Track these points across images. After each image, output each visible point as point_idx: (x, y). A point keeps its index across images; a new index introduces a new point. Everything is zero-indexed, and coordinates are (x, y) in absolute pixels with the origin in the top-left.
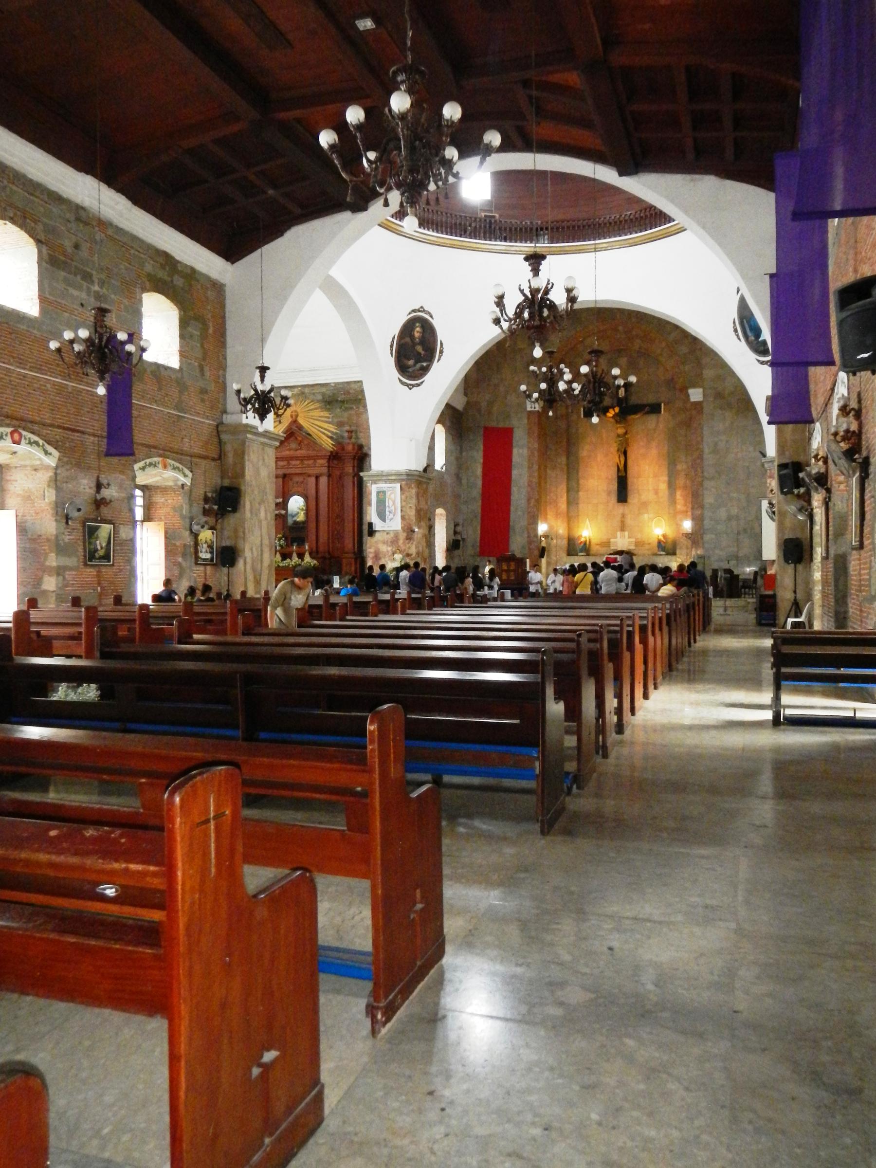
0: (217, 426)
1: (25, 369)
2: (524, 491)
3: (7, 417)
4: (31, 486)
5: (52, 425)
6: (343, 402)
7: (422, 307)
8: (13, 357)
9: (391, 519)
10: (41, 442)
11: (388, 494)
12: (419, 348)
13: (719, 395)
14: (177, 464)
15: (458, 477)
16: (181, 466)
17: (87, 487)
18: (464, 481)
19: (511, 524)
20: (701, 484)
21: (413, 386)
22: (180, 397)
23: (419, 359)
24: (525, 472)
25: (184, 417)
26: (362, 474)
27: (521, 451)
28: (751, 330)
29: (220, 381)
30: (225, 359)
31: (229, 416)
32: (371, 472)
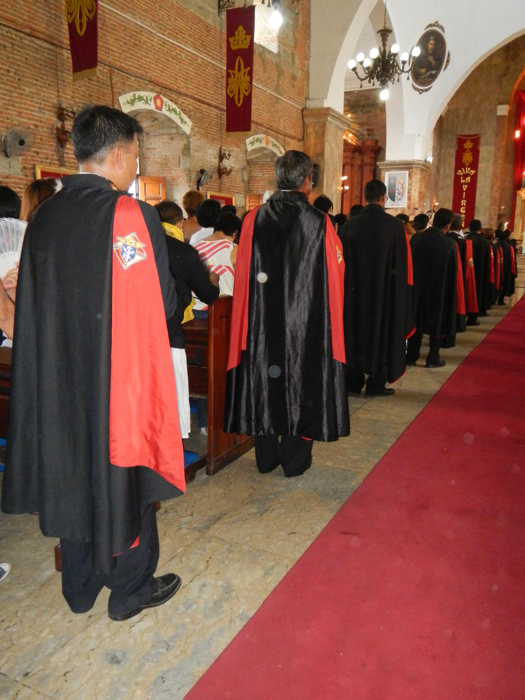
0: (302, 110)
1: (164, 35)
2: (489, 181)
3: (151, 81)
4: (168, 154)
5: (186, 95)
6: (363, 106)
7: (437, 22)
8: (155, 22)
9: (400, 199)
10: (178, 110)
11: (398, 179)
12: (431, 59)
15: (438, 169)
16: (278, 144)
17: (212, 157)
18: (442, 171)
19: (476, 205)
21: (423, 91)
22: (278, 81)
23: (430, 67)
24: (491, 164)
25: (281, 99)
26: (378, 163)
27: (489, 147)
29: (305, 69)
30: (309, 50)
31: (311, 102)
32: (385, 162)
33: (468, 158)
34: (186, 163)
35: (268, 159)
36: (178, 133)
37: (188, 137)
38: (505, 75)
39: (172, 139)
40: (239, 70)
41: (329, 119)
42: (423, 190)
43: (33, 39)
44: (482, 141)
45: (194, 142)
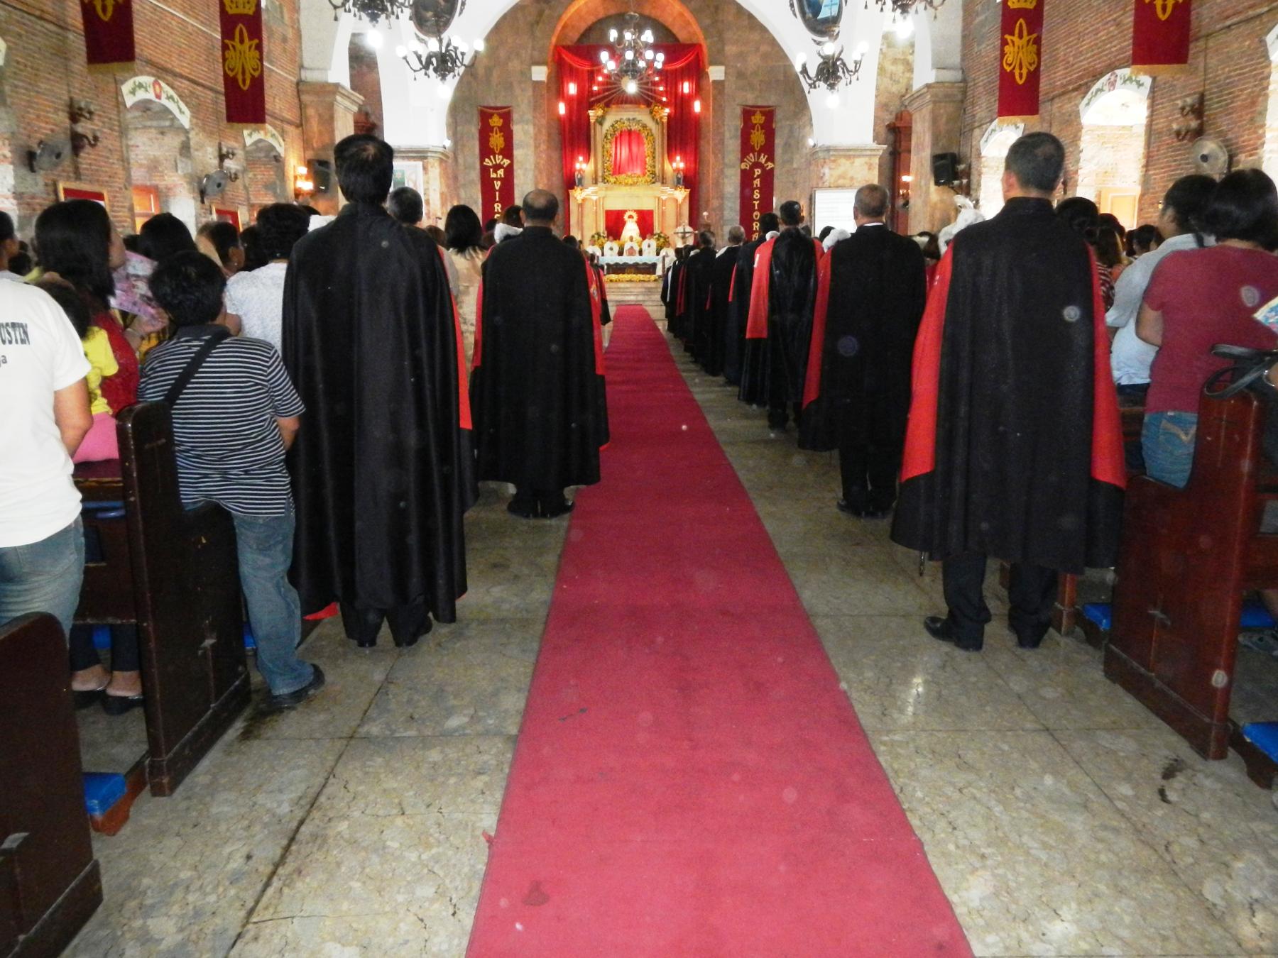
0: (298, 84)
4: (157, 153)
10: (176, 97)
13: (741, 75)
14: (274, 132)
18: (461, 161)
20: (722, 171)
28: (809, 6)
33: (497, 141)
34: (185, 167)
35: (262, 155)
36: (171, 126)
37: (186, 132)
38: (537, 23)
39: (162, 133)
40: (242, 41)
41: (338, 98)
42: (445, 189)
43: (42, 23)
44: (515, 116)
45: (195, 138)
